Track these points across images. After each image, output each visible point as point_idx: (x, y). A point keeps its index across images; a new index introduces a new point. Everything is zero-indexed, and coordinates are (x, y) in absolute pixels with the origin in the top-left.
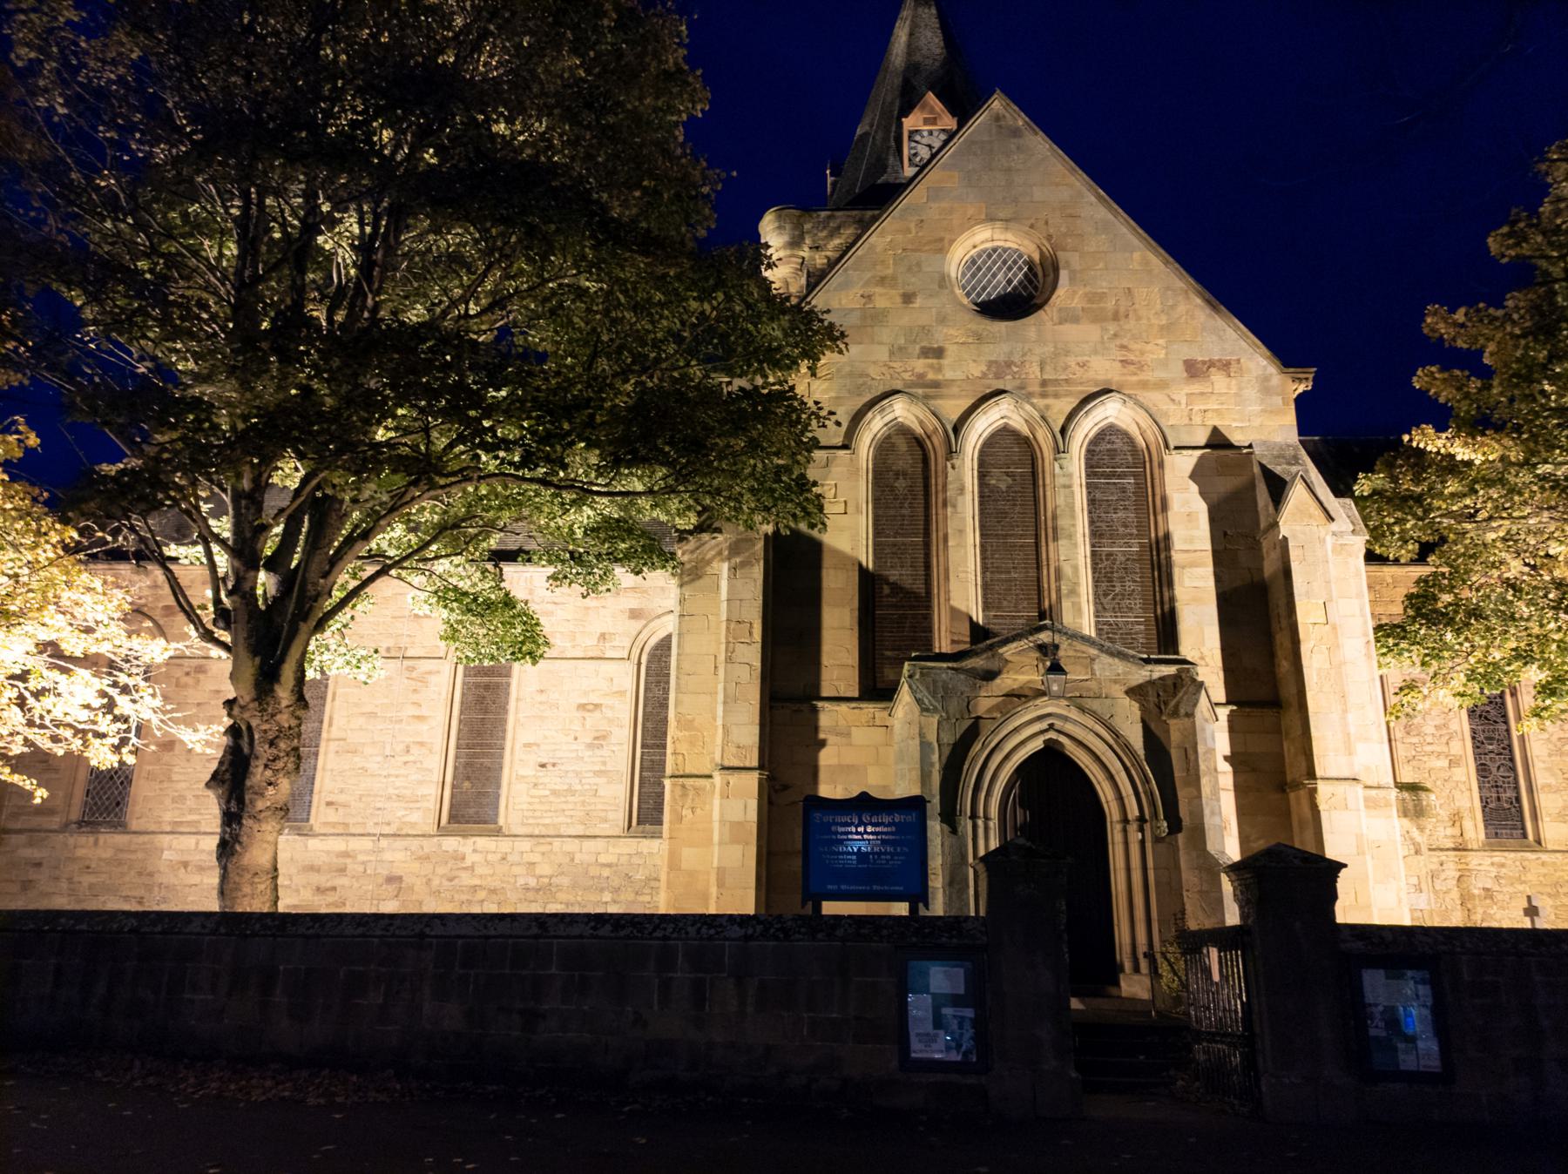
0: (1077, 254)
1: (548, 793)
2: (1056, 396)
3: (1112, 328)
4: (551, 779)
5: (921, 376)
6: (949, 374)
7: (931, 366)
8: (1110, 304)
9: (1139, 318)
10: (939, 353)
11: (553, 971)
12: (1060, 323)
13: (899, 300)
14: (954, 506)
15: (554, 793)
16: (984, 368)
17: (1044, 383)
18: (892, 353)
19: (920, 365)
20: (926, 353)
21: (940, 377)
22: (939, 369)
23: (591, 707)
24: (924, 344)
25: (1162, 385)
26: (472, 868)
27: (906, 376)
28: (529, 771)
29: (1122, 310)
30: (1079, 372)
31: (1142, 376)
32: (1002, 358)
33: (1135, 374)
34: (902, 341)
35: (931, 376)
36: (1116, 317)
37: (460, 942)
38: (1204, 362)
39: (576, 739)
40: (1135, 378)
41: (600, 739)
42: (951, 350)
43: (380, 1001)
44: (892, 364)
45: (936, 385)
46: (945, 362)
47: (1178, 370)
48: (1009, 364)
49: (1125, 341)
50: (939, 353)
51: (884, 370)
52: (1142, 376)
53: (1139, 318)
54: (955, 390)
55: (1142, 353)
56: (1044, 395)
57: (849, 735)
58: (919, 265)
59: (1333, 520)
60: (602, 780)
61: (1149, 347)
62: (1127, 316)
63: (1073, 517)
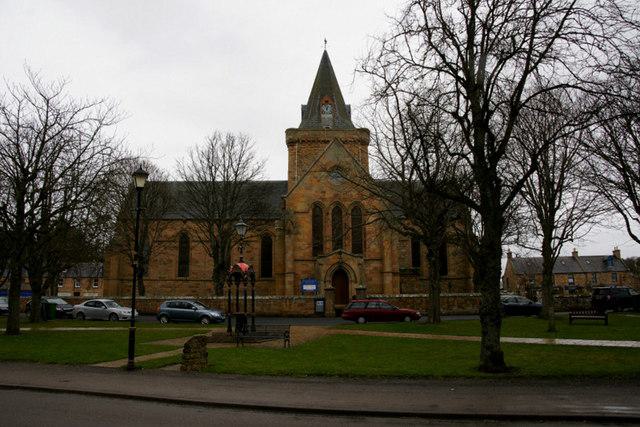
6: (327, 196)
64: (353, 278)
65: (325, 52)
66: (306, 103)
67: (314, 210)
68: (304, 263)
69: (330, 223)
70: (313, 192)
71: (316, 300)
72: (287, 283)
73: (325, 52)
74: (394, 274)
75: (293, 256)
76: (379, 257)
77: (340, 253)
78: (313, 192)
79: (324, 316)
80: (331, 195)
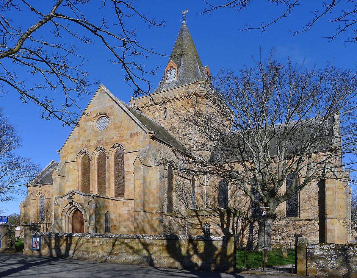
2: (108, 145)
3: (118, 130)
5: (87, 145)
10: (89, 141)
19: (86, 143)
25: (126, 140)
30: (112, 140)
31: (123, 139)
40: (121, 139)
45: (89, 147)
47: (129, 136)
48: (100, 140)
50: (89, 141)
52: (123, 139)
56: (106, 146)
62: (120, 127)
78: (81, 142)
80: (95, 143)
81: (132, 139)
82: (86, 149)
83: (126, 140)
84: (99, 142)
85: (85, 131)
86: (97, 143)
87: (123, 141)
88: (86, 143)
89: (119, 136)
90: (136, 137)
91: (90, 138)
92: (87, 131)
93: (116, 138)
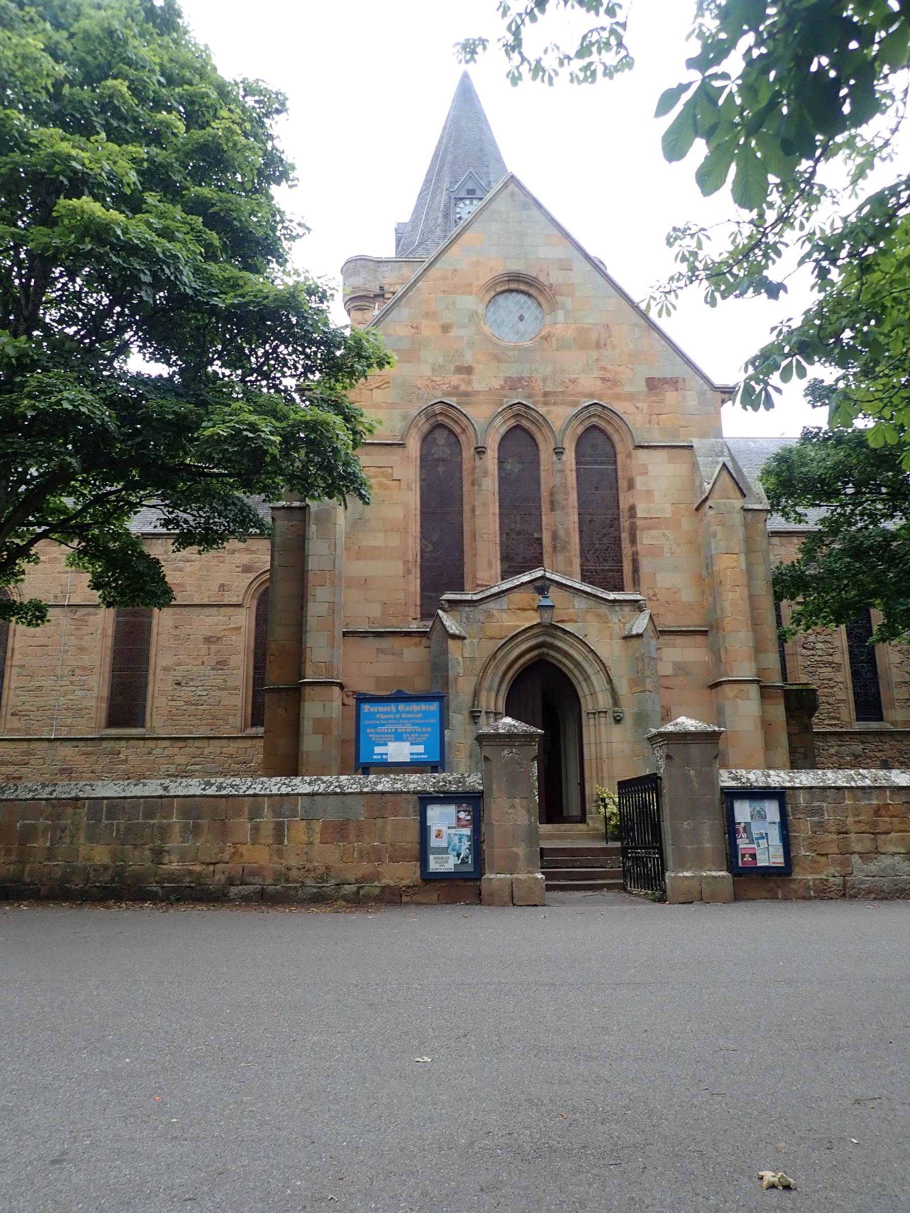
0: (570, 299)
1: (183, 703)
2: (555, 404)
3: (594, 354)
4: (185, 693)
5: (456, 388)
6: (476, 387)
7: (463, 380)
8: (594, 336)
9: (614, 347)
11: (175, 820)
12: (557, 350)
13: (439, 330)
14: (480, 485)
15: (187, 703)
16: (502, 383)
17: (546, 394)
18: (434, 370)
19: (455, 379)
20: (460, 370)
21: (470, 389)
22: (470, 382)
23: (214, 639)
24: (458, 363)
26: (126, 761)
27: (445, 387)
28: (169, 686)
29: (602, 341)
30: (571, 386)
32: (515, 375)
33: (610, 388)
34: (441, 361)
35: (463, 388)
36: (598, 346)
37: (105, 802)
38: (659, 379)
39: (203, 662)
40: (611, 392)
41: (221, 664)
42: (478, 368)
43: (48, 844)
44: (434, 379)
45: (467, 394)
46: (474, 377)
47: (642, 387)
48: (520, 379)
49: (603, 364)
50: (469, 370)
51: (428, 382)
52: (617, 390)
53: (614, 347)
54: (481, 398)
55: (617, 374)
56: (546, 404)
57: (402, 654)
58: (454, 303)
59: (745, 496)
60: (225, 693)
61: (621, 369)
62: (605, 345)
63: (566, 493)
64: (604, 701)
65: (466, 76)
66: (406, 217)
67: (427, 439)
68: (384, 643)
69: (490, 485)
70: (426, 371)
71: (425, 799)
72: (307, 726)
73: (466, 76)
74: (765, 691)
75: (333, 609)
76: (693, 621)
77: (541, 587)
78: (426, 371)
79: (478, 898)
80: (496, 384)
81: (654, 398)
82: (452, 401)
83: (630, 397)
84: (513, 384)
85: (446, 328)
86: (502, 388)
87: (617, 397)
88: (455, 379)
89: (603, 380)
90: (671, 396)
91: (468, 359)
92: (455, 332)
93: (589, 382)
